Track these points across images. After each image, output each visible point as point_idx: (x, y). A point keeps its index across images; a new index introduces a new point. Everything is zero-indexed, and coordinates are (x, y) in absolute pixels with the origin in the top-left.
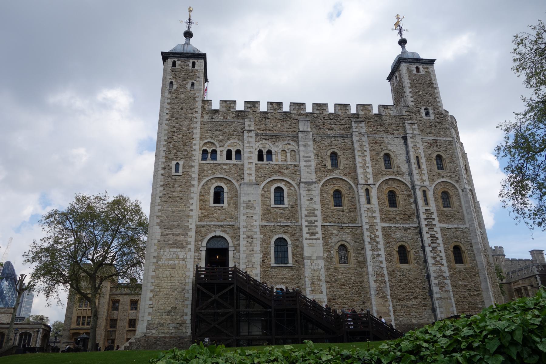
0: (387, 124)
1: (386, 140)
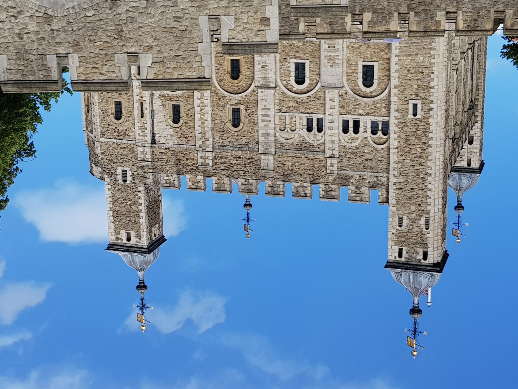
0: (172, 163)
1: (174, 140)
